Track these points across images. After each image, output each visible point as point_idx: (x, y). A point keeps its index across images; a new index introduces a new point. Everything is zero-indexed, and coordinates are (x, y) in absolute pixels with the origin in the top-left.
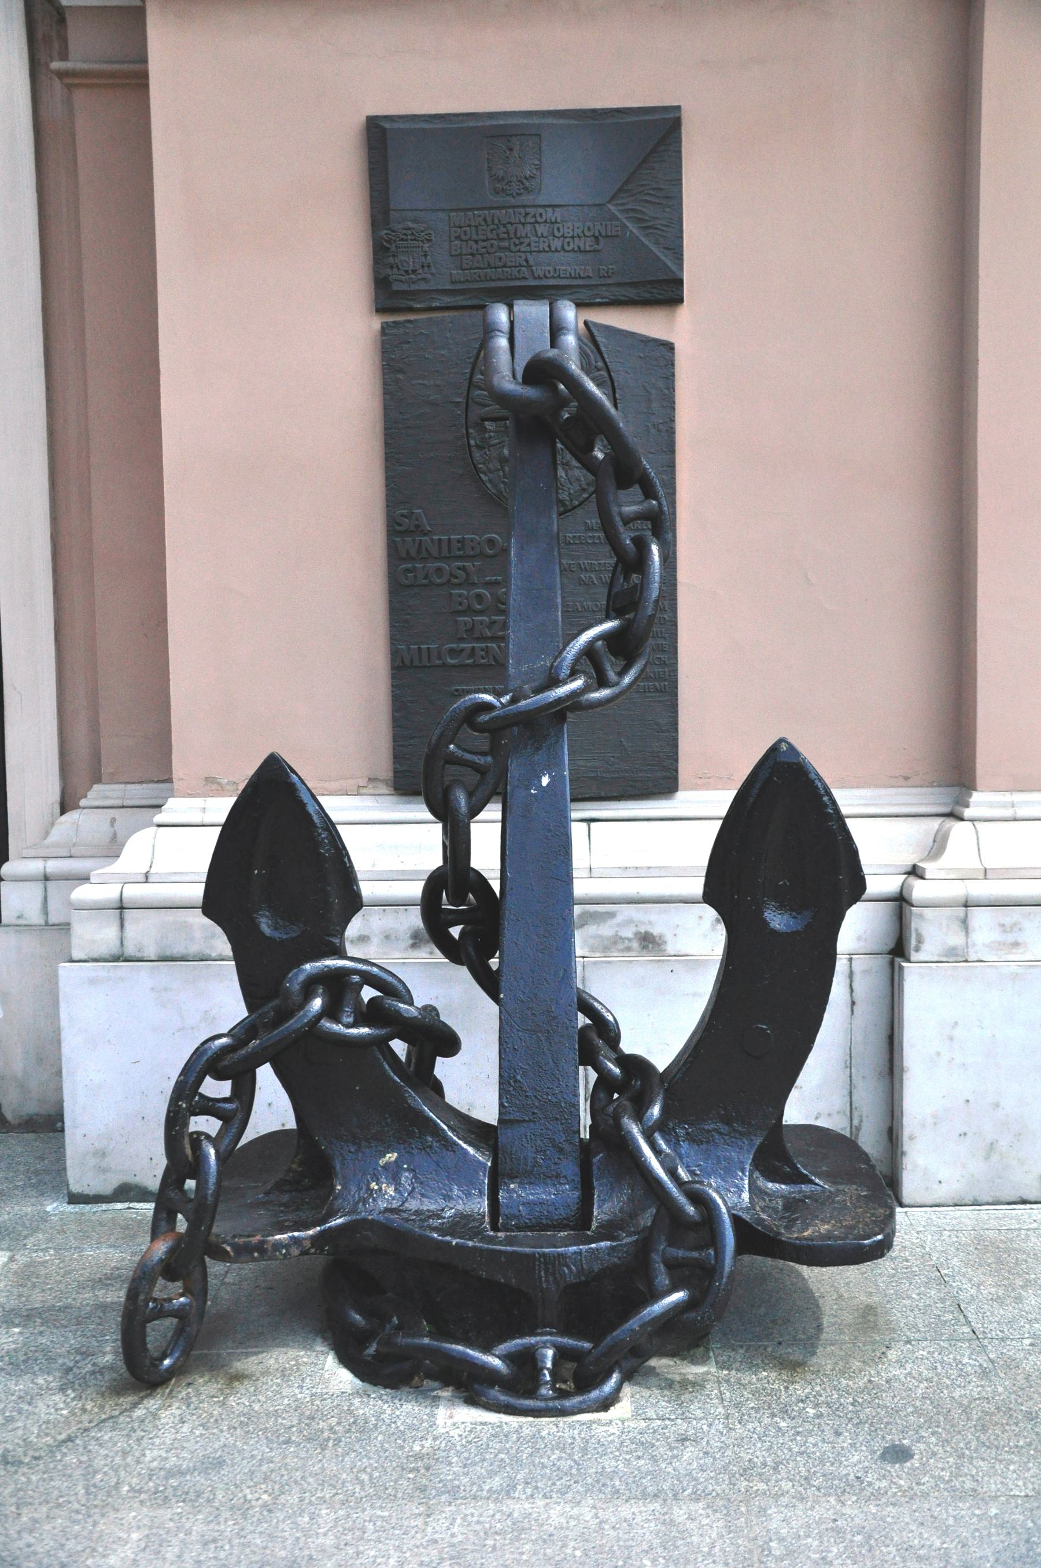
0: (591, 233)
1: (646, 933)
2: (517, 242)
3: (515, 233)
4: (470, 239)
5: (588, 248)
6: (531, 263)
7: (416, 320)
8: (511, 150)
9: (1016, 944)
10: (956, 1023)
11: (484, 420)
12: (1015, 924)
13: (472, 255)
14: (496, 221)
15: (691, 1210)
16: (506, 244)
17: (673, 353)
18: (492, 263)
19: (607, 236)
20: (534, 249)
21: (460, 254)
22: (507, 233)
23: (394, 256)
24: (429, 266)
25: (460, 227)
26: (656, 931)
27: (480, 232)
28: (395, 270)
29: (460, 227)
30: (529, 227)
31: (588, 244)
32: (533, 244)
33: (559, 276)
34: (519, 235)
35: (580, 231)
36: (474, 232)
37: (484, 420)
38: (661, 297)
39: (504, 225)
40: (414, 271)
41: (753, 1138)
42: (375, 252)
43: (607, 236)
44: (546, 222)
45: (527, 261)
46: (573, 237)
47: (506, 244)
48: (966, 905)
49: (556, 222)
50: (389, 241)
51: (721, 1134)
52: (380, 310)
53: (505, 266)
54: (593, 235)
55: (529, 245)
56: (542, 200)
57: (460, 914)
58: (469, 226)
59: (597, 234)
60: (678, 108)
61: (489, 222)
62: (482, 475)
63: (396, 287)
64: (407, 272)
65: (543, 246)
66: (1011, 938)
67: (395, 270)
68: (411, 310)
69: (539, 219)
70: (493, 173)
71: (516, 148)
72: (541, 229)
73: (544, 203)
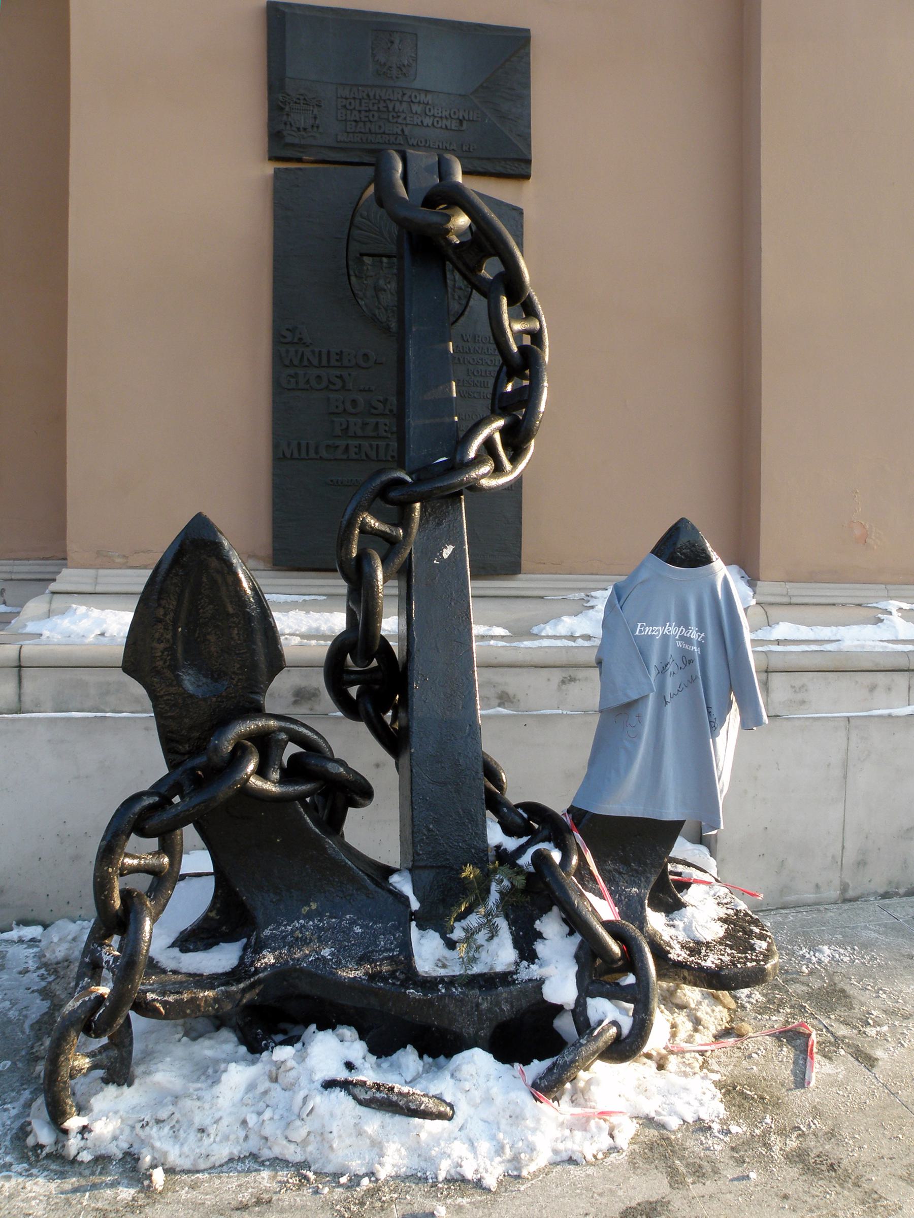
0: (456, 117)
1: (503, 692)
2: (395, 115)
3: (394, 109)
4: (354, 109)
5: (453, 128)
6: (406, 133)
7: (305, 169)
8: (392, 42)
9: (803, 702)
10: (760, 766)
11: (362, 255)
12: (803, 686)
13: (356, 121)
14: (377, 97)
15: (616, 948)
16: (384, 116)
17: (522, 217)
18: (373, 130)
19: (469, 120)
20: (408, 122)
21: (346, 120)
22: (387, 107)
23: (288, 115)
24: (318, 127)
25: (346, 99)
26: (511, 691)
27: (363, 104)
28: (288, 127)
29: (346, 99)
30: (405, 105)
31: (454, 125)
32: (408, 118)
33: (429, 147)
34: (396, 110)
35: (447, 114)
36: (358, 104)
37: (362, 255)
38: (512, 172)
39: (385, 101)
40: (305, 129)
41: (649, 875)
42: (271, 110)
43: (469, 120)
44: (419, 102)
45: (403, 131)
46: (441, 117)
47: (384, 116)
48: (766, 672)
49: (428, 104)
50: (284, 103)
51: (620, 873)
52: (273, 158)
53: (384, 133)
54: (458, 118)
55: (405, 118)
56: (417, 84)
57: (368, 677)
58: (354, 98)
59: (461, 118)
60: (528, 31)
61: (372, 97)
62: (359, 301)
63: (289, 140)
64: (299, 129)
65: (417, 120)
66: (799, 697)
67: (288, 127)
68: (300, 160)
69: (414, 100)
70: (376, 58)
71: (397, 41)
72: (415, 108)
73: (419, 87)
